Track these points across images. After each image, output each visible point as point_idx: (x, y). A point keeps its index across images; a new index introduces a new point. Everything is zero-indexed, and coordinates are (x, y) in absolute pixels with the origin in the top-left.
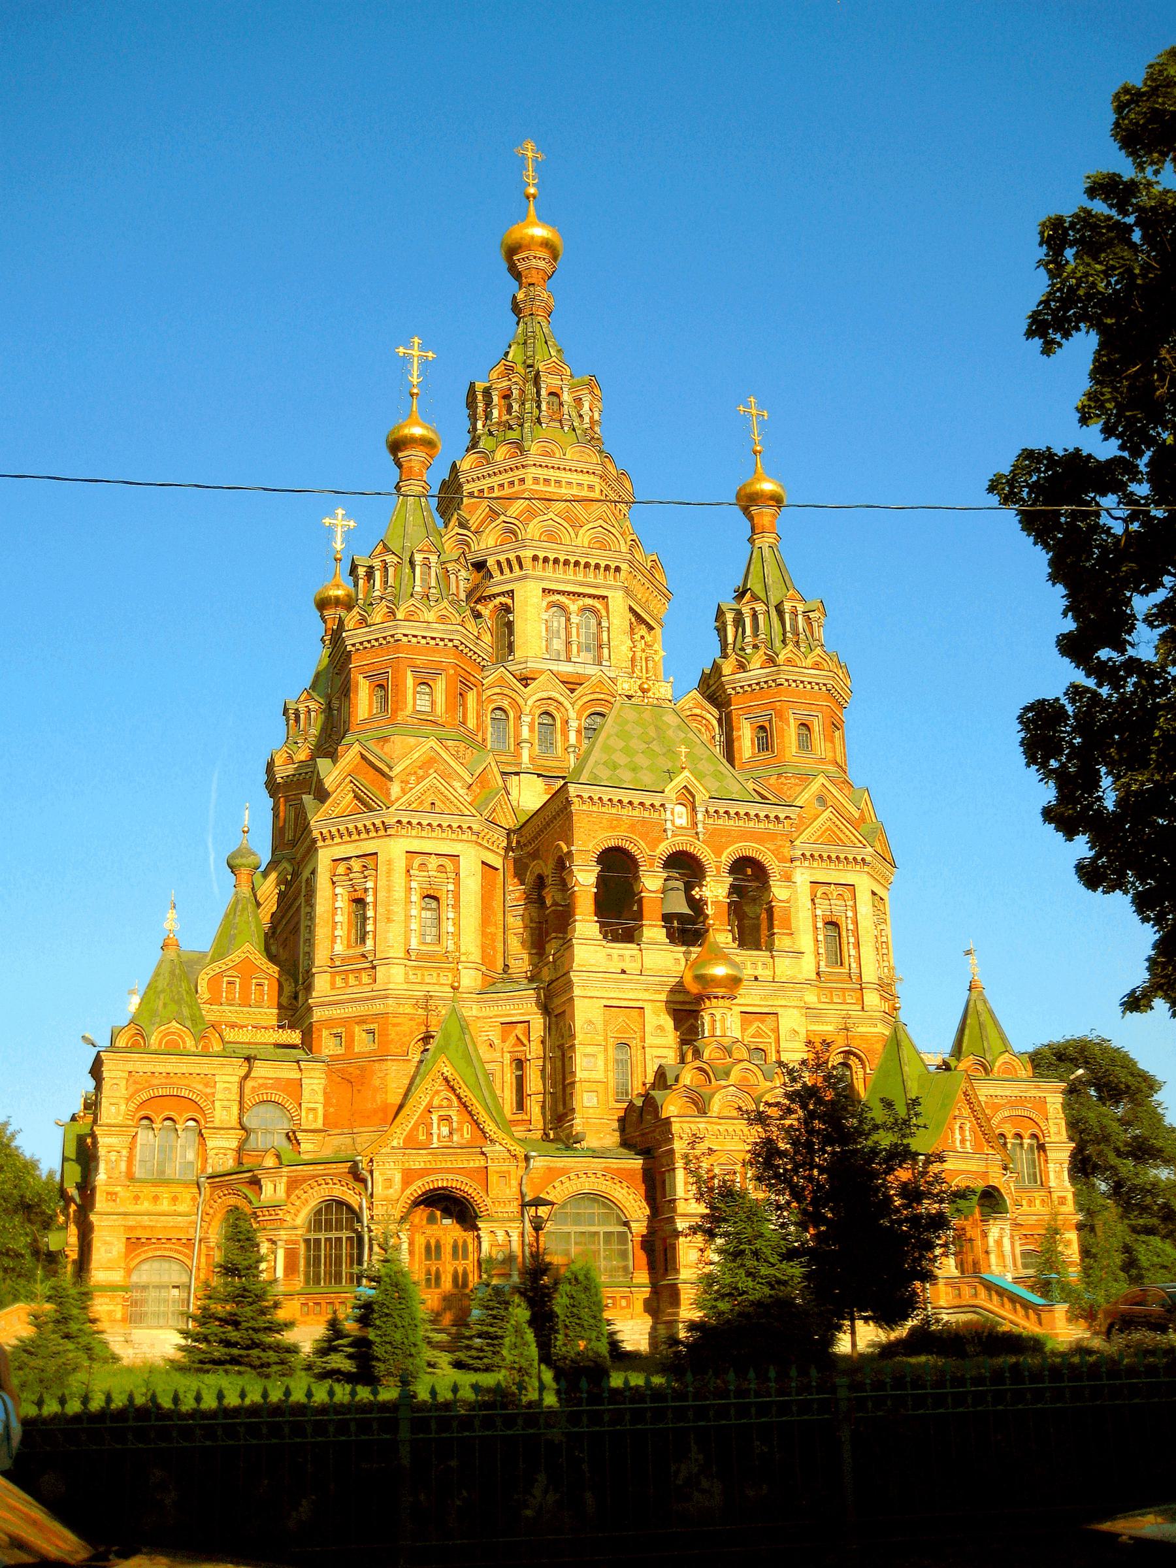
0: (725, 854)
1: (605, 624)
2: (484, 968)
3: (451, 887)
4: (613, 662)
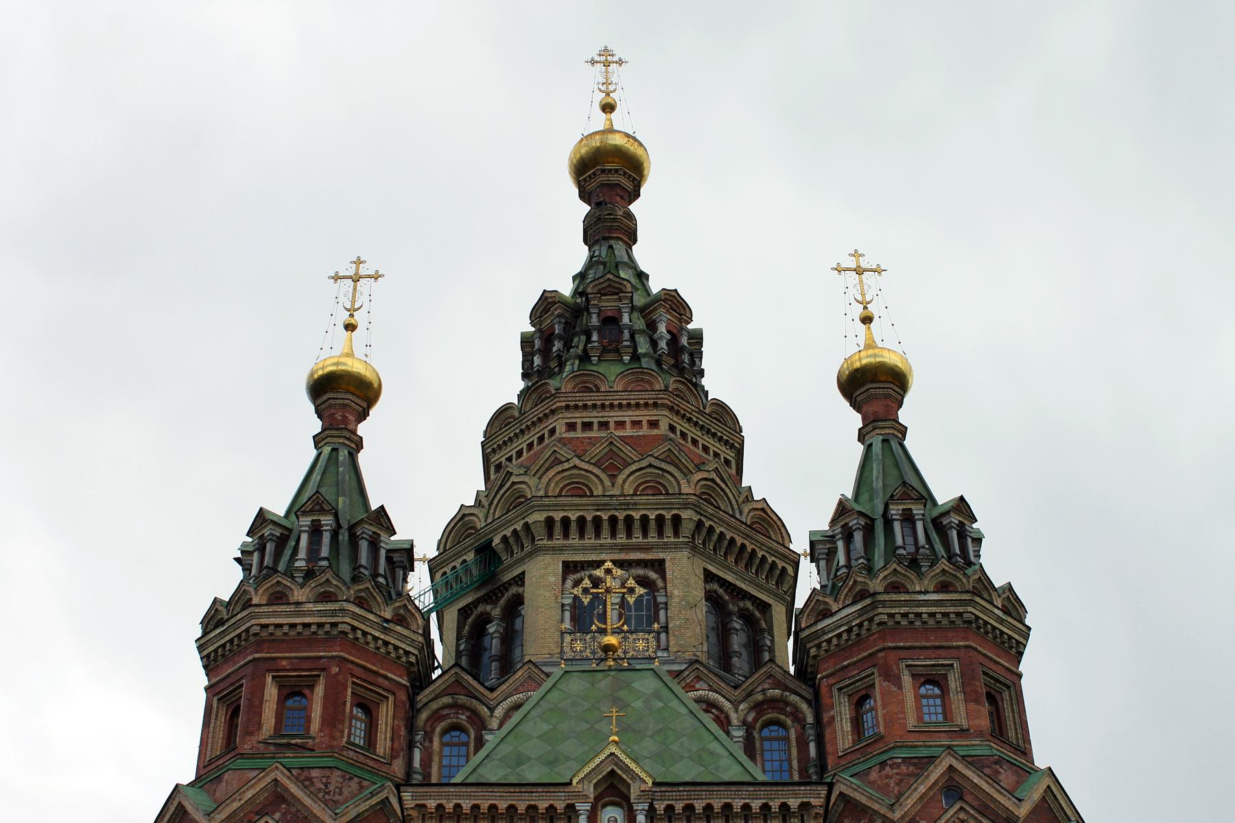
1: (661, 599)
4: (673, 649)
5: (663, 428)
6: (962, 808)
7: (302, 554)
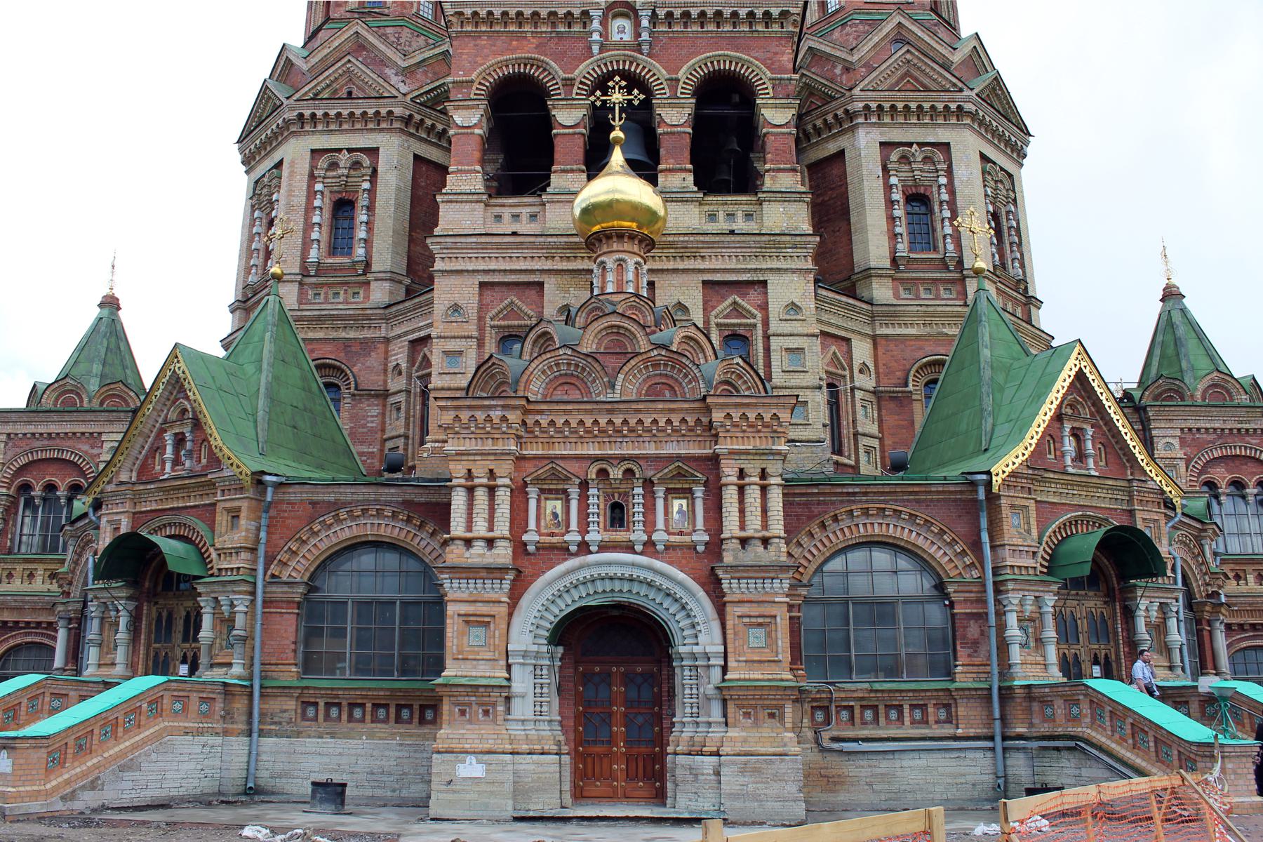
0: (685, 68)
2: (408, 281)
3: (366, 185)
6: (908, 51)
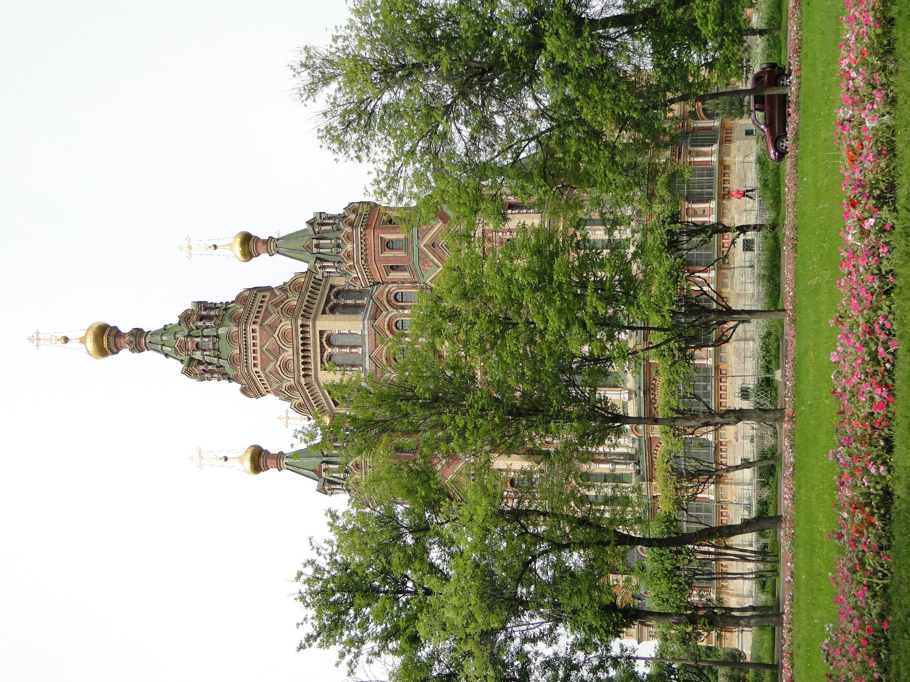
5: (256, 327)
7: (338, 475)
